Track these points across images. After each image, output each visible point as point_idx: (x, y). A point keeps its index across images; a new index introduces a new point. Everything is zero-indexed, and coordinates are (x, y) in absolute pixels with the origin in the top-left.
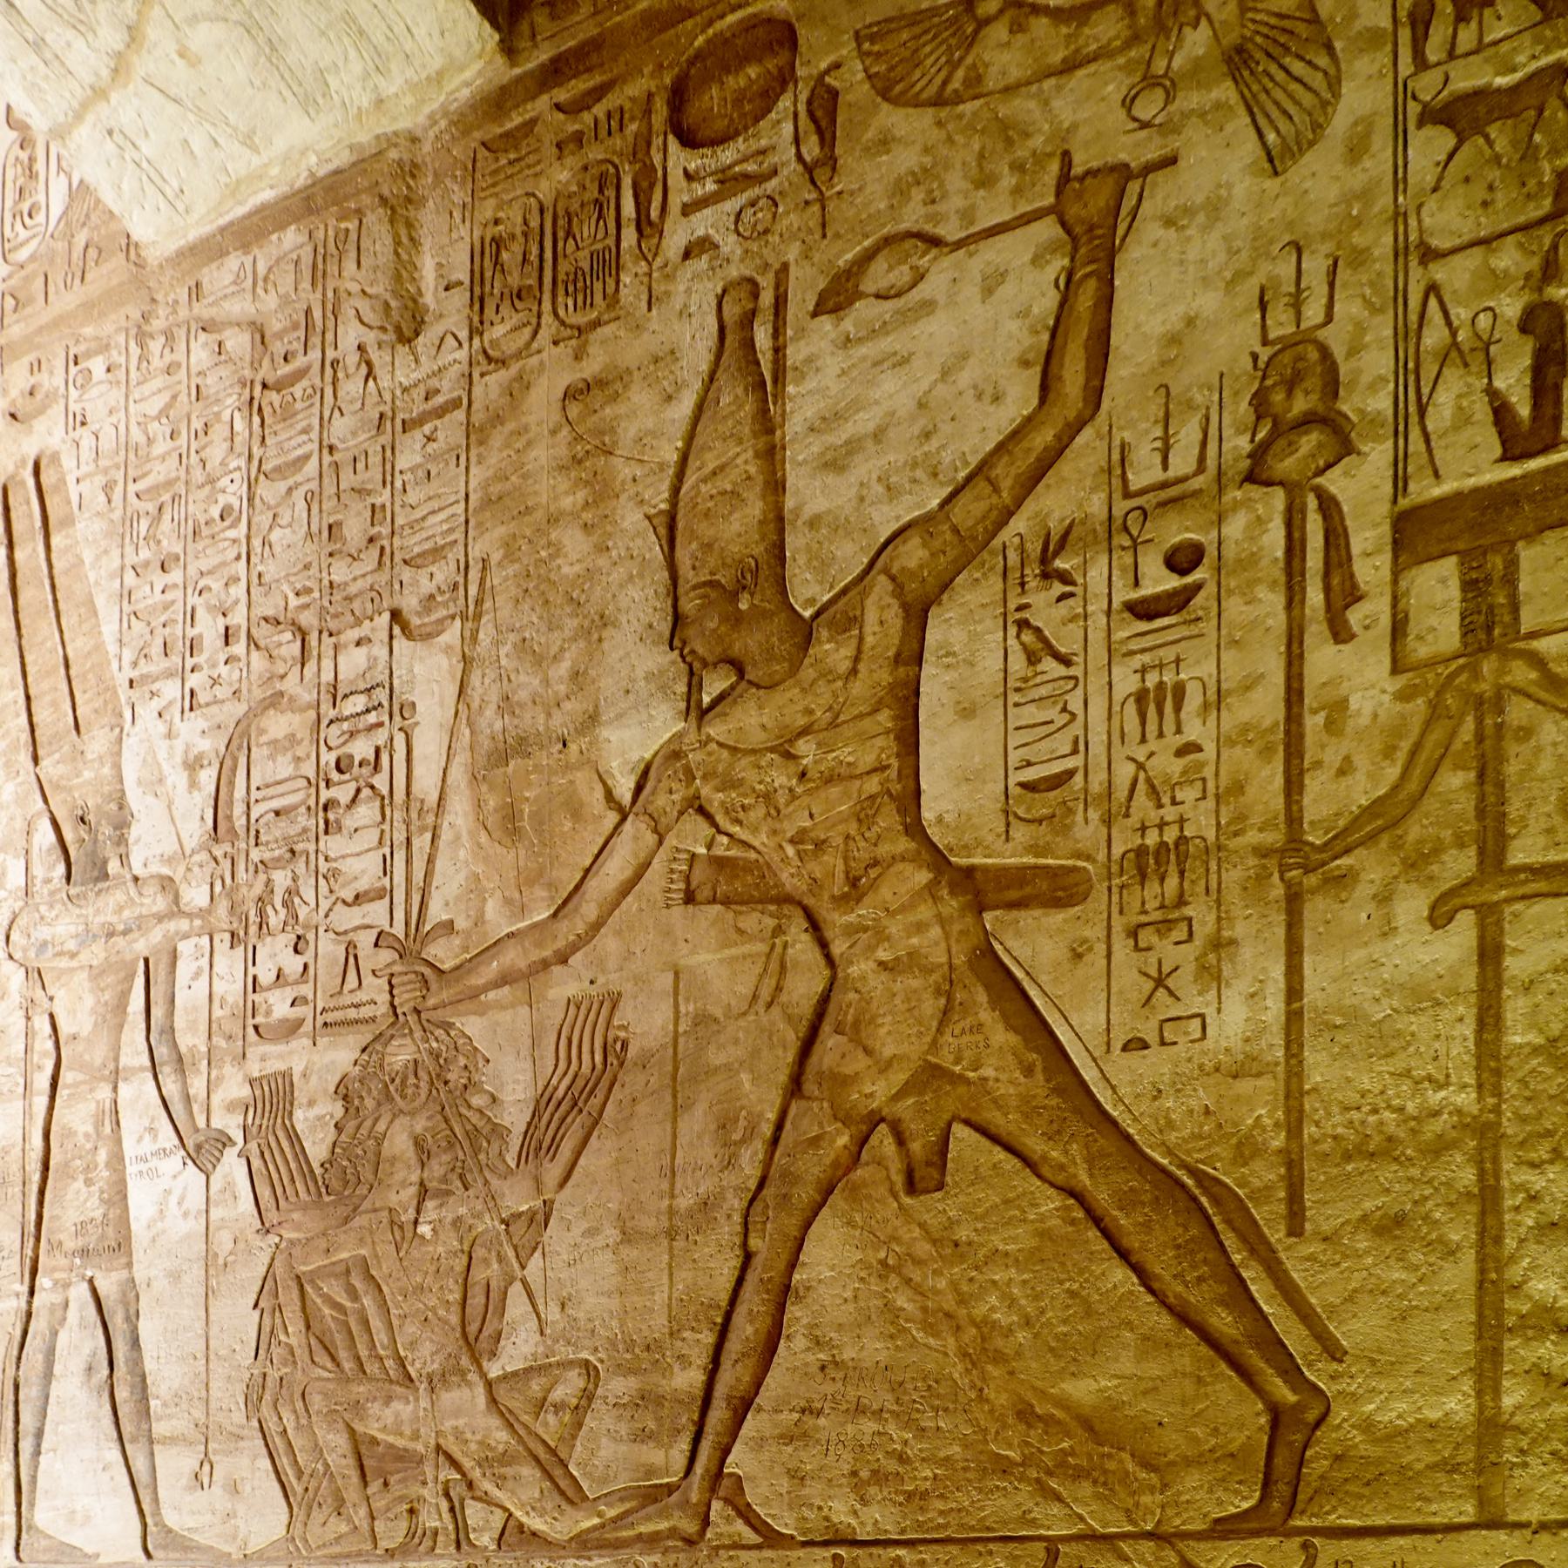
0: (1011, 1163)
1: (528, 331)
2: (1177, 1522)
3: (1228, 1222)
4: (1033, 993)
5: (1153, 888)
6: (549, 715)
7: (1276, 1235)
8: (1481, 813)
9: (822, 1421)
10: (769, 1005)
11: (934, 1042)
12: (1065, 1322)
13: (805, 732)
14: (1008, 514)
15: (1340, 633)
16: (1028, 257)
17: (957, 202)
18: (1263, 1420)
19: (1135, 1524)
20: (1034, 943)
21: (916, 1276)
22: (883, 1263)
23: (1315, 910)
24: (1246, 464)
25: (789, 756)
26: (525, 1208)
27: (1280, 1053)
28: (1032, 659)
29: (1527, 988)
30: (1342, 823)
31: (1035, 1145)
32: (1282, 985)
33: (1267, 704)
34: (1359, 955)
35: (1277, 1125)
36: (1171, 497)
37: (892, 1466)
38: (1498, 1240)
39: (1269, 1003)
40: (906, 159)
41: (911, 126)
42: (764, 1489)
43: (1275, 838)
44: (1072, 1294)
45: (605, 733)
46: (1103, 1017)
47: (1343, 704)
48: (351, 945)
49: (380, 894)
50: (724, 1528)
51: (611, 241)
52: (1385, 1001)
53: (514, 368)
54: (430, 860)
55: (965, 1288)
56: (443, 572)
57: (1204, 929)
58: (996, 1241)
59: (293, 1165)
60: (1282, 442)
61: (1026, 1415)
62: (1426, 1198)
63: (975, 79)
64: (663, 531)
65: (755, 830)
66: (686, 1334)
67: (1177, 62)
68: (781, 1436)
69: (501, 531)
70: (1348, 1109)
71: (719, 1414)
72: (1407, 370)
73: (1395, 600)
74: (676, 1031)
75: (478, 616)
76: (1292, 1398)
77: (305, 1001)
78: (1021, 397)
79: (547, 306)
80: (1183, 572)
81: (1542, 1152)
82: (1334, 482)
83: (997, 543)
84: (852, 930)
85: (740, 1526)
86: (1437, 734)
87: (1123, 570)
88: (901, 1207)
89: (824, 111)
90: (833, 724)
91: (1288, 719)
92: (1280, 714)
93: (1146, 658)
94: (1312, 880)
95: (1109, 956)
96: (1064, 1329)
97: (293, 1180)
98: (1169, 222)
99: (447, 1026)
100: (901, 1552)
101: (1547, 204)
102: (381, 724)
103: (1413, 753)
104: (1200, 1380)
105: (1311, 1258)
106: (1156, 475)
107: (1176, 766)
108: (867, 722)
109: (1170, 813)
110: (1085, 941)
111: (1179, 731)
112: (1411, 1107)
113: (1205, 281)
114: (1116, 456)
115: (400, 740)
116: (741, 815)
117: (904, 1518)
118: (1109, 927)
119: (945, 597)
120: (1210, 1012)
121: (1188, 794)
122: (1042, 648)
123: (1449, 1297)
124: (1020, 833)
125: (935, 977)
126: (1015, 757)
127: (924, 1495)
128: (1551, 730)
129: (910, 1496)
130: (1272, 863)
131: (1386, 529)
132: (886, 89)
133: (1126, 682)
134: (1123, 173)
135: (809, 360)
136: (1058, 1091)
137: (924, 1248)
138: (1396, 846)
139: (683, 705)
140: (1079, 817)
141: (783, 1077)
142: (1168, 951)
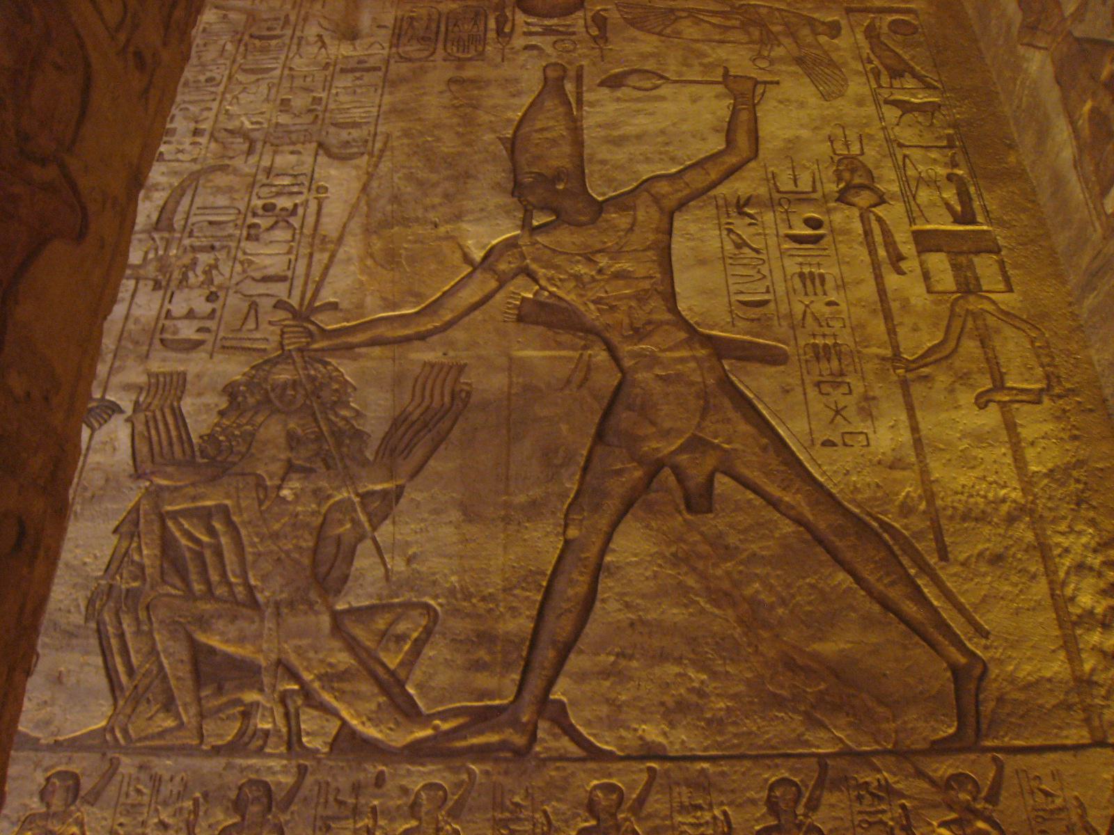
0: (758, 501)
1: (426, 53)
2: (908, 742)
3: (903, 550)
4: (760, 407)
5: (824, 365)
6: (426, 210)
7: (933, 560)
8: (988, 360)
9: (635, 664)
10: (580, 387)
11: (699, 425)
12: (810, 603)
13: (600, 251)
14: (714, 185)
15: (900, 272)
16: (713, 94)
17: (673, 68)
18: (949, 674)
19: (878, 743)
20: (758, 383)
21: (700, 565)
22: (674, 555)
23: (917, 390)
24: (837, 195)
25: (590, 260)
26: (378, 487)
27: (913, 459)
28: (738, 246)
29: (1032, 444)
30: (920, 352)
31: (774, 490)
32: (907, 423)
33: (868, 290)
34: (943, 416)
35: (920, 497)
36: (802, 198)
37: (694, 698)
38: (1056, 572)
39: (902, 432)
40: (647, 49)
41: (648, 43)
42: (587, 714)
43: (888, 352)
44: (812, 586)
45: (465, 226)
46: (807, 427)
47: (907, 300)
48: (254, 306)
49: (282, 279)
50: (553, 744)
51: (481, 34)
52: (965, 441)
53: (418, 64)
54: (327, 268)
55: (736, 576)
56: (355, 133)
57: (859, 387)
58: (754, 547)
59: (174, 433)
60: (853, 191)
61: (791, 665)
62: (1012, 546)
63: (678, 34)
64: (508, 145)
65: (569, 293)
66: (517, 592)
67: (773, 54)
68: (600, 673)
69: (402, 124)
70: (956, 493)
71: (547, 654)
72: (904, 180)
73: (922, 264)
74: (509, 394)
75: (380, 157)
76: (963, 660)
77: (208, 330)
78: (716, 144)
79: (440, 46)
80: (814, 228)
81: (1063, 527)
82: (879, 211)
83: (712, 193)
84: (634, 355)
85: (566, 744)
86: (957, 324)
87: (783, 220)
88: (685, 520)
89: (601, 22)
90: (619, 252)
91: (881, 301)
92: (876, 297)
93: (800, 260)
94: (910, 376)
95: (805, 394)
96: (809, 608)
97: (171, 444)
98: (780, 102)
99: (326, 364)
100: (705, 765)
101: (945, 143)
102: (301, 193)
103: (948, 327)
104: (905, 647)
105: (955, 575)
106: (794, 189)
107: (827, 310)
108: (640, 254)
109: (827, 330)
110: (789, 385)
111: (825, 294)
112: (991, 495)
113: (802, 126)
114: (770, 176)
115: (313, 206)
116: (559, 283)
117: (706, 737)
118: (803, 380)
119: (684, 209)
120: (870, 431)
121: (837, 325)
122: (741, 244)
123: (1039, 603)
124: (740, 324)
125: (693, 390)
126: (733, 288)
127: (720, 722)
128: (1009, 331)
129: (709, 722)
130: (888, 365)
131: (909, 234)
132: (632, 23)
133: (792, 267)
134: (756, 83)
135: (598, 101)
136: (785, 463)
137: (704, 548)
138: (950, 368)
139: (520, 223)
140: (776, 323)
141: (593, 431)
142: (838, 396)
